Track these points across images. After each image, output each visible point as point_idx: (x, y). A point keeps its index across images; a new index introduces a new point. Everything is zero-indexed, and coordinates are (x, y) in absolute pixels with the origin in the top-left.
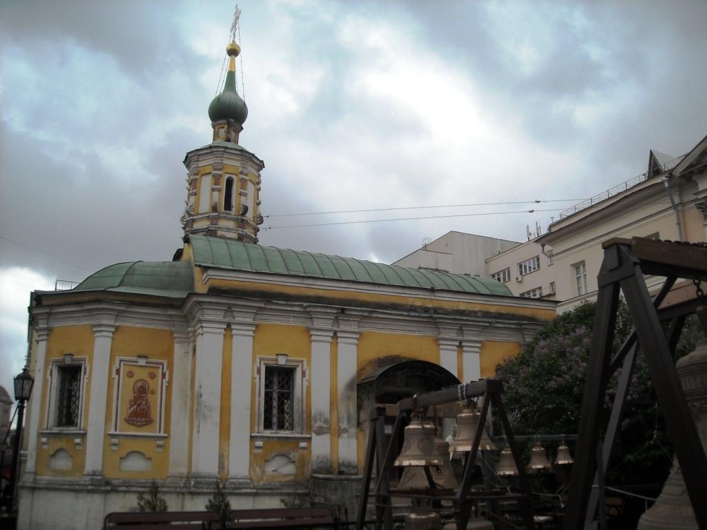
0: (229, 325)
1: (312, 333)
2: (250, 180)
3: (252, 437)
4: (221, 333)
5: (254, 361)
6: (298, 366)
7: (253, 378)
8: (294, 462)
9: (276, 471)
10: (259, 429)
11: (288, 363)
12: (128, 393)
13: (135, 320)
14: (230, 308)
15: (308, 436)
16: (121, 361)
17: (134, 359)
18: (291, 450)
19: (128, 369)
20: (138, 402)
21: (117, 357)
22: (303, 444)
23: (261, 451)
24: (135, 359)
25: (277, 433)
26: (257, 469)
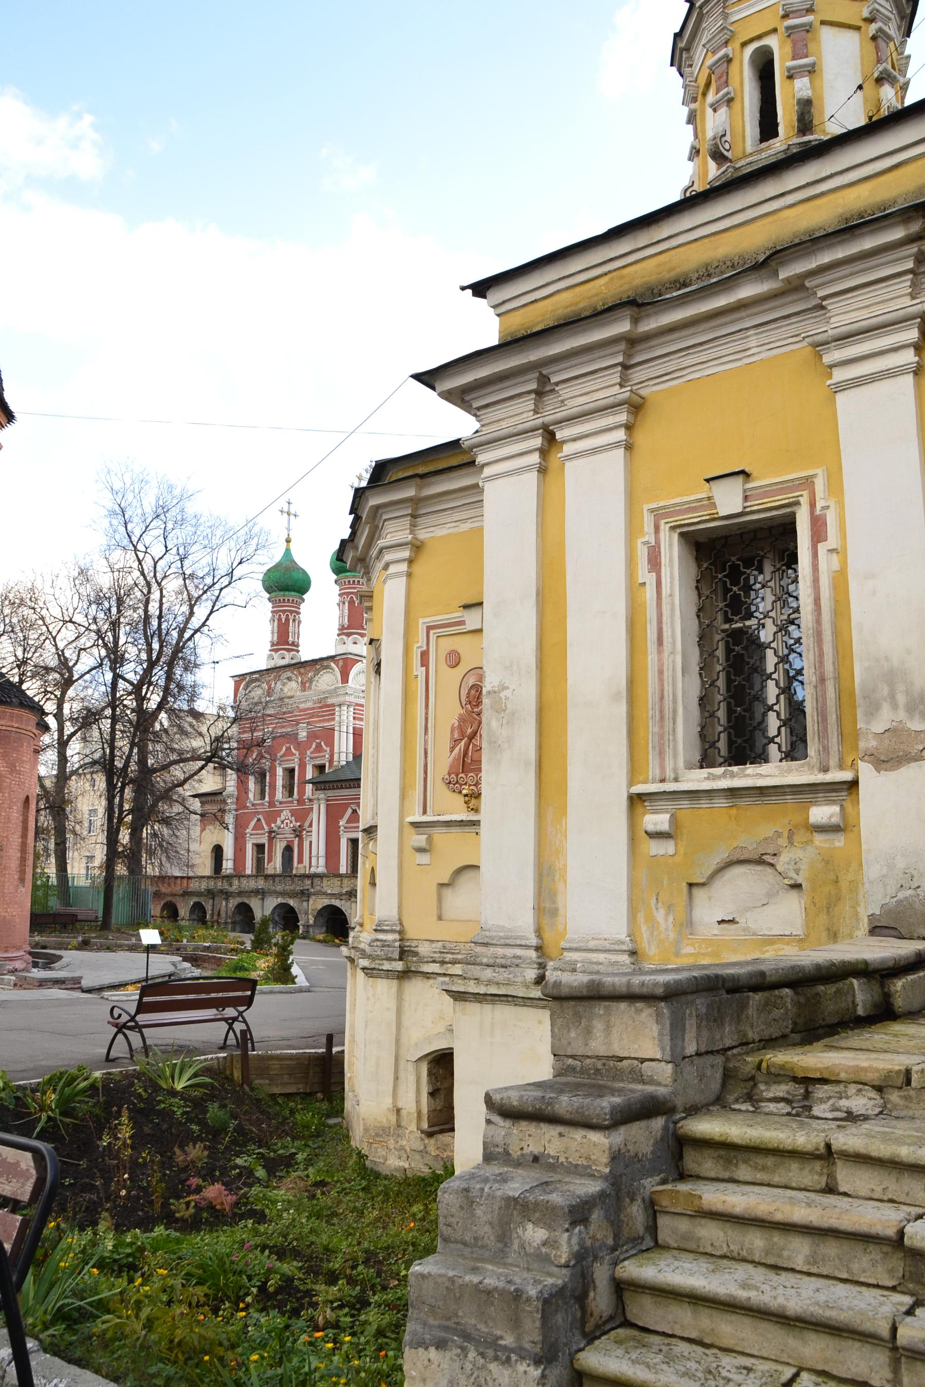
0: (550, 436)
1: (829, 358)
2: (823, 23)
3: (636, 801)
4: (526, 469)
5: (632, 530)
6: (797, 503)
7: (634, 588)
8: (797, 886)
9: (732, 921)
10: (662, 767)
11: (755, 505)
12: (449, 711)
13: (458, 516)
14: (544, 380)
15: (847, 776)
16: (429, 628)
17: (458, 615)
18: (783, 841)
19: (447, 644)
20: (469, 731)
21: (421, 621)
22: (822, 813)
23: (668, 847)
24: (458, 615)
25: (733, 775)
26: (660, 915)
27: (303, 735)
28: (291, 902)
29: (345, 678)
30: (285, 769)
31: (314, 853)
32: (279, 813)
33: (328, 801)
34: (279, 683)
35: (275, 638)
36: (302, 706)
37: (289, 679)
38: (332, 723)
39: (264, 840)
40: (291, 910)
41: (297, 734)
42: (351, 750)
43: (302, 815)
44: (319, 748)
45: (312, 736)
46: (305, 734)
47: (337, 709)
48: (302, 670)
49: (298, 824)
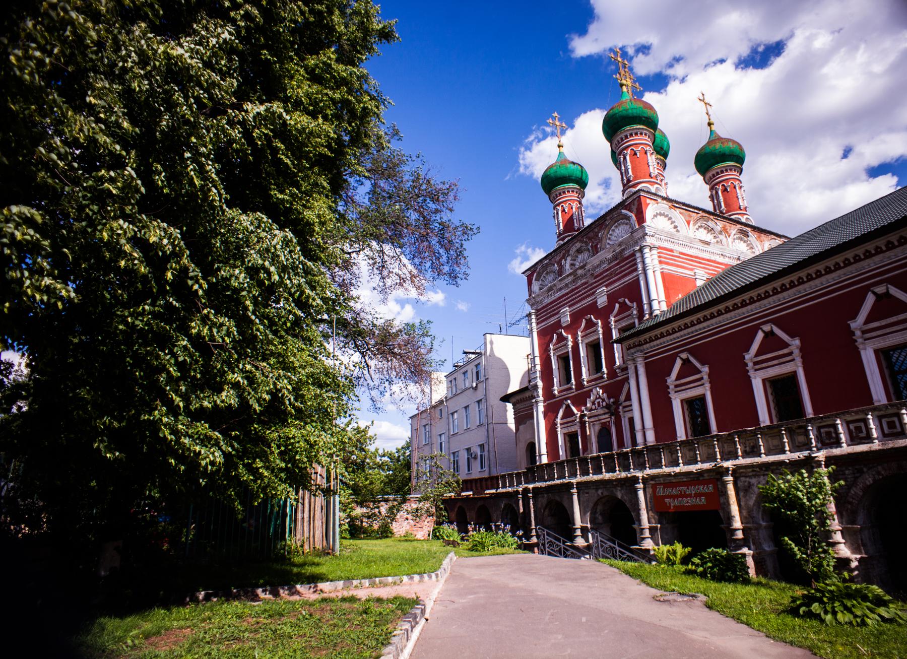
27: (602, 301)
28: (619, 495)
29: (641, 219)
30: (588, 345)
31: (638, 426)
32: (588, 394)
33: (646, 358)
34: (569, 259)
35: (562, 228)
36: (598, 271)
37: (579, 251)
38: (635, 274)
39: (576, 428)
40: (620, 503)
41: (596, 302)
42: (662, 297)
43: (616, 388)
44: (624, 308)
45: (612, 298)
46: (605, 299)
47: (638, 255)
48: (591, 235)
49: (612, 400)
